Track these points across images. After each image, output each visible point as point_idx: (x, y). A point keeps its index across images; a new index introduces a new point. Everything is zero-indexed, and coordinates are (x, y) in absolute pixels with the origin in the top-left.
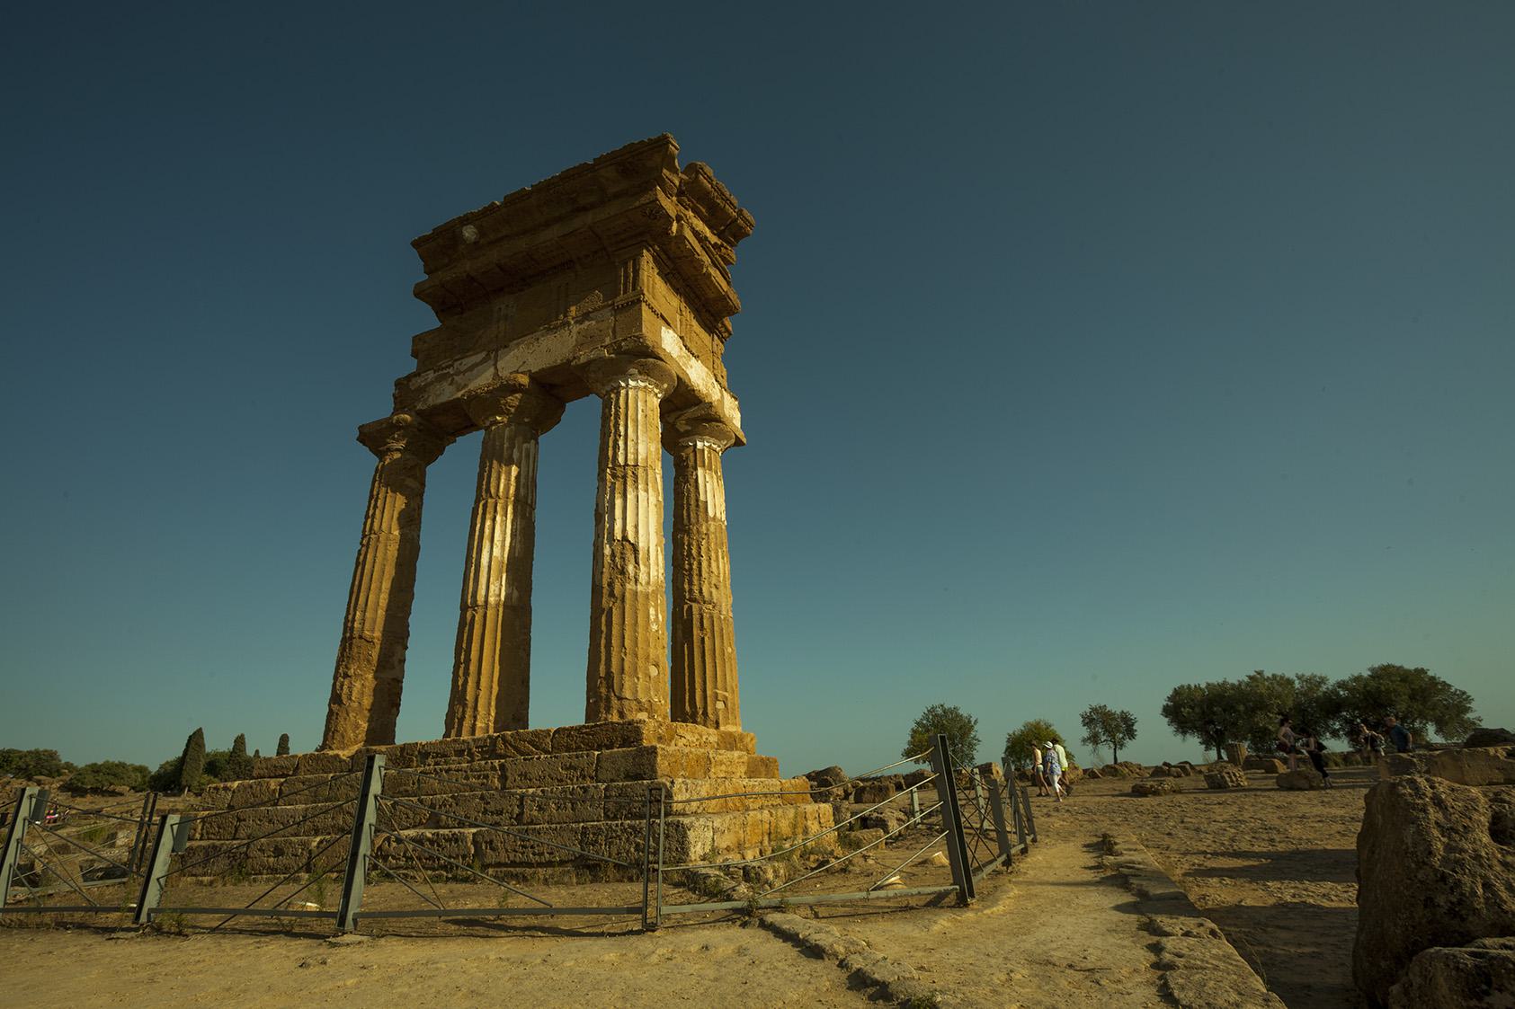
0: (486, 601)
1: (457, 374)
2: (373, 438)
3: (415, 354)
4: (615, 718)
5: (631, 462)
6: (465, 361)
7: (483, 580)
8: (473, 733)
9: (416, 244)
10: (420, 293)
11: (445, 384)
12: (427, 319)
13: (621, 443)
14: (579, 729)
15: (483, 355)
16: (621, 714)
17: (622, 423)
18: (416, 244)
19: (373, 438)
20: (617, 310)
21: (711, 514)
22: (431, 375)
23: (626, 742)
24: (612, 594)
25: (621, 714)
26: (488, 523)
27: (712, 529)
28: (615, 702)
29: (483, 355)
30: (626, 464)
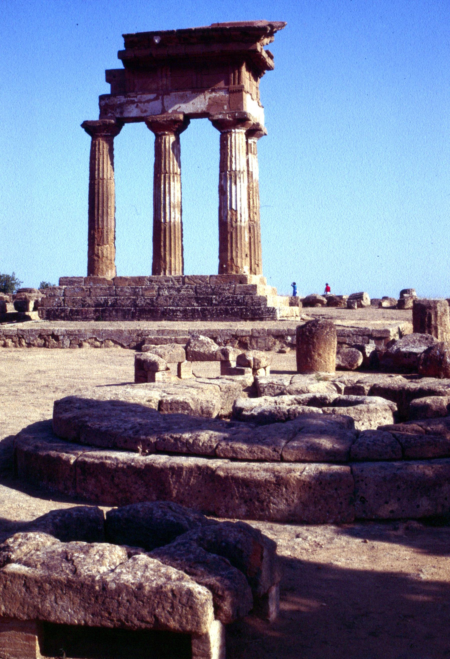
0: (170, 221)
1: (141, 102)
2: (88, 126)
3: (108, 80)
4: (234, 273)
5: (238, 170)
6: (145, 96)
7: (167, 211)
8: (171, 274)
9: (124, 36)
10: (121, 55)
11: (133, 106)
12: (119, 65)
13: (233, 159)
14: (216, 277)
15: (155, 95)
16: (237, 272)
17: (233, 150)
18: (124, 36)
19: (88, 126)
20: (230, 92)
21: (254, 178)
22: (122, 99)
23: (241, 283)
24: (232, 226)
25: (237, 272)
26: (167, 186)
27: (254, 186)
28: (234, 268)
29: (155, 95)
30: (236, 170)
